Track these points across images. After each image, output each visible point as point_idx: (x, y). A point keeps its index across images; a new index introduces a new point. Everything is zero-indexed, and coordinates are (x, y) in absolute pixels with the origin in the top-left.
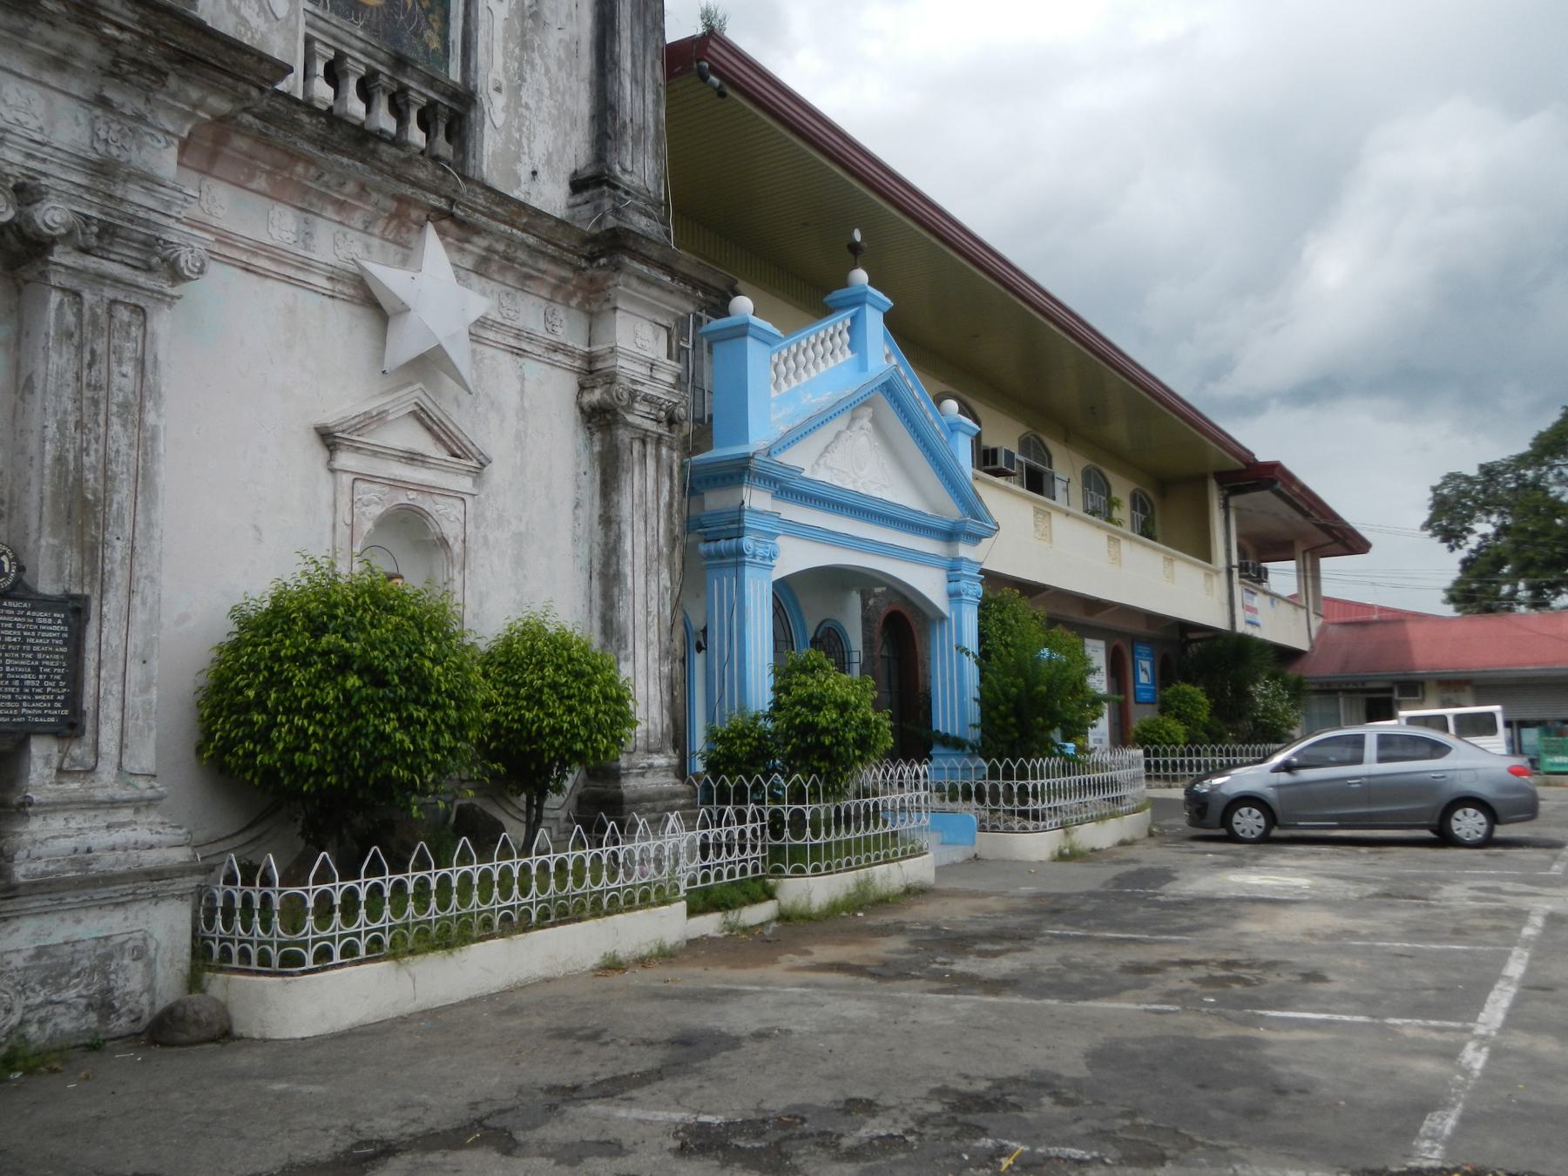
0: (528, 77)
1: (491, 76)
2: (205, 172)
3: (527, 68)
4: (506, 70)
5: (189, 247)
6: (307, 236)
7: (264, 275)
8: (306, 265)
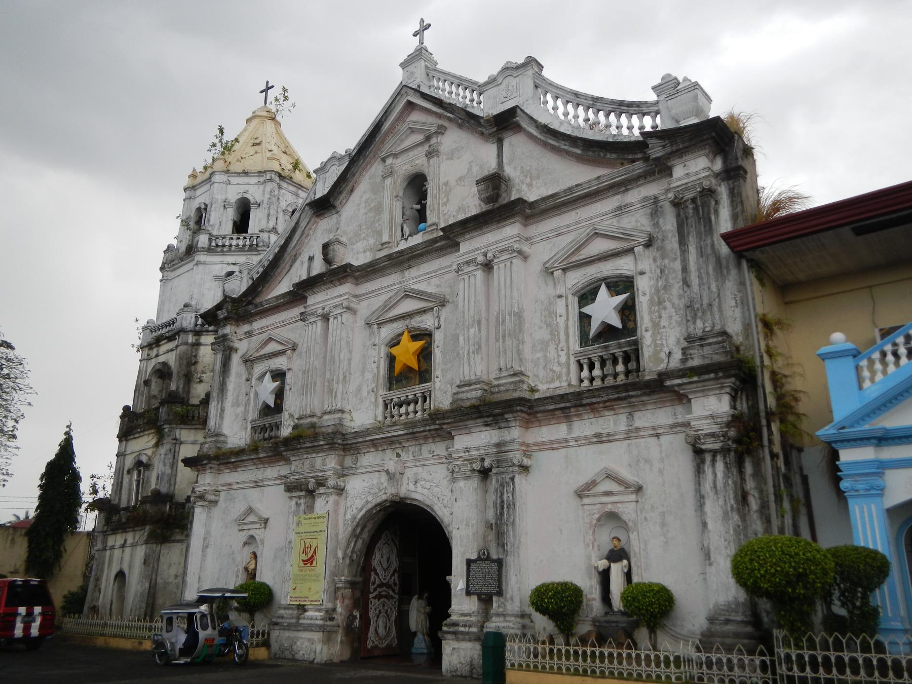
0: (663, 315)
1: (643, 328)
2: (540, 426)
3: (663, 312)
4: (651, 320)
5: (516, 456)
6: (570, 429)
7: (557, 449)
8: (566, 441)
